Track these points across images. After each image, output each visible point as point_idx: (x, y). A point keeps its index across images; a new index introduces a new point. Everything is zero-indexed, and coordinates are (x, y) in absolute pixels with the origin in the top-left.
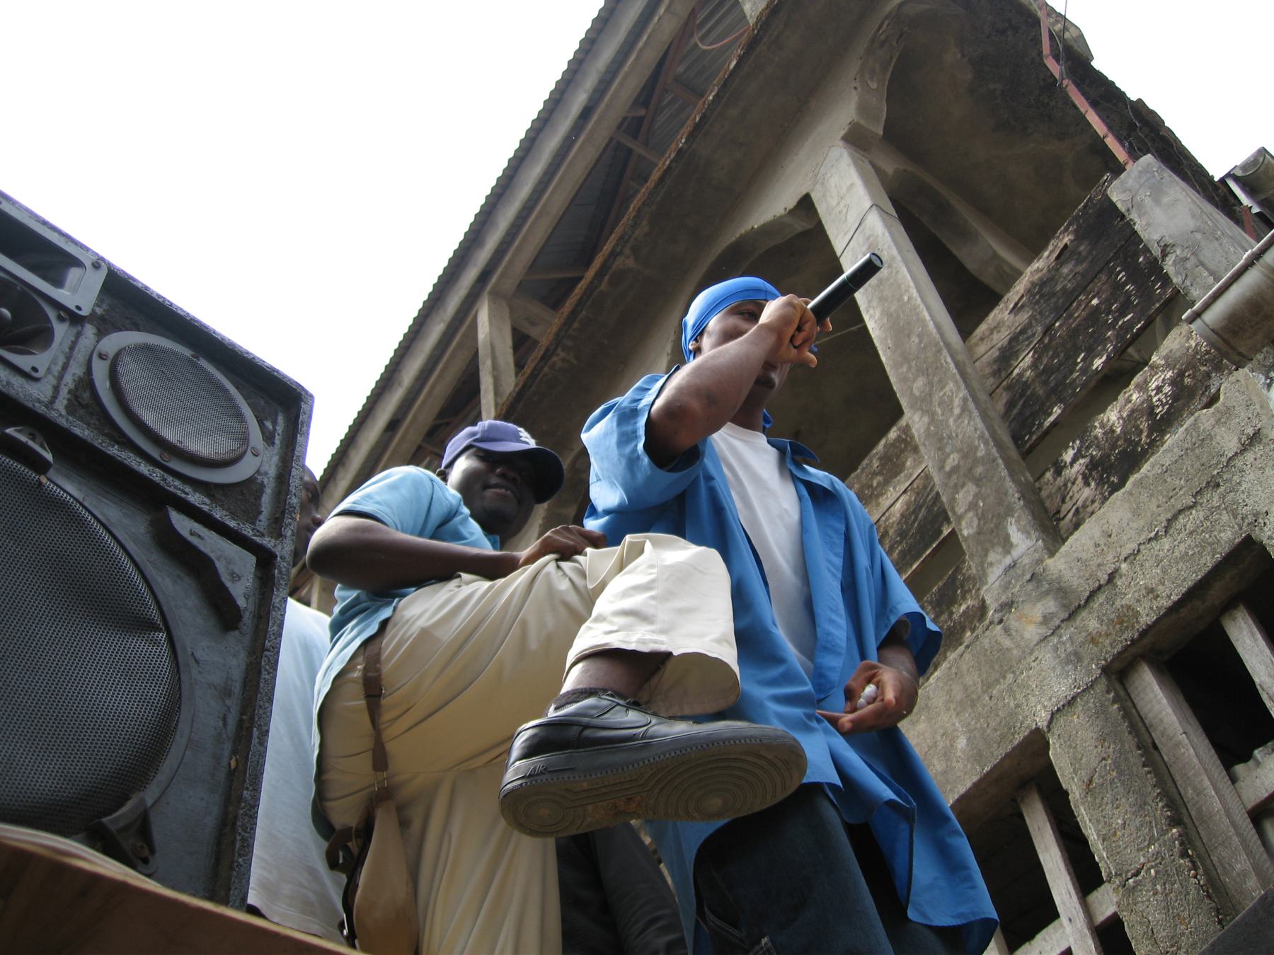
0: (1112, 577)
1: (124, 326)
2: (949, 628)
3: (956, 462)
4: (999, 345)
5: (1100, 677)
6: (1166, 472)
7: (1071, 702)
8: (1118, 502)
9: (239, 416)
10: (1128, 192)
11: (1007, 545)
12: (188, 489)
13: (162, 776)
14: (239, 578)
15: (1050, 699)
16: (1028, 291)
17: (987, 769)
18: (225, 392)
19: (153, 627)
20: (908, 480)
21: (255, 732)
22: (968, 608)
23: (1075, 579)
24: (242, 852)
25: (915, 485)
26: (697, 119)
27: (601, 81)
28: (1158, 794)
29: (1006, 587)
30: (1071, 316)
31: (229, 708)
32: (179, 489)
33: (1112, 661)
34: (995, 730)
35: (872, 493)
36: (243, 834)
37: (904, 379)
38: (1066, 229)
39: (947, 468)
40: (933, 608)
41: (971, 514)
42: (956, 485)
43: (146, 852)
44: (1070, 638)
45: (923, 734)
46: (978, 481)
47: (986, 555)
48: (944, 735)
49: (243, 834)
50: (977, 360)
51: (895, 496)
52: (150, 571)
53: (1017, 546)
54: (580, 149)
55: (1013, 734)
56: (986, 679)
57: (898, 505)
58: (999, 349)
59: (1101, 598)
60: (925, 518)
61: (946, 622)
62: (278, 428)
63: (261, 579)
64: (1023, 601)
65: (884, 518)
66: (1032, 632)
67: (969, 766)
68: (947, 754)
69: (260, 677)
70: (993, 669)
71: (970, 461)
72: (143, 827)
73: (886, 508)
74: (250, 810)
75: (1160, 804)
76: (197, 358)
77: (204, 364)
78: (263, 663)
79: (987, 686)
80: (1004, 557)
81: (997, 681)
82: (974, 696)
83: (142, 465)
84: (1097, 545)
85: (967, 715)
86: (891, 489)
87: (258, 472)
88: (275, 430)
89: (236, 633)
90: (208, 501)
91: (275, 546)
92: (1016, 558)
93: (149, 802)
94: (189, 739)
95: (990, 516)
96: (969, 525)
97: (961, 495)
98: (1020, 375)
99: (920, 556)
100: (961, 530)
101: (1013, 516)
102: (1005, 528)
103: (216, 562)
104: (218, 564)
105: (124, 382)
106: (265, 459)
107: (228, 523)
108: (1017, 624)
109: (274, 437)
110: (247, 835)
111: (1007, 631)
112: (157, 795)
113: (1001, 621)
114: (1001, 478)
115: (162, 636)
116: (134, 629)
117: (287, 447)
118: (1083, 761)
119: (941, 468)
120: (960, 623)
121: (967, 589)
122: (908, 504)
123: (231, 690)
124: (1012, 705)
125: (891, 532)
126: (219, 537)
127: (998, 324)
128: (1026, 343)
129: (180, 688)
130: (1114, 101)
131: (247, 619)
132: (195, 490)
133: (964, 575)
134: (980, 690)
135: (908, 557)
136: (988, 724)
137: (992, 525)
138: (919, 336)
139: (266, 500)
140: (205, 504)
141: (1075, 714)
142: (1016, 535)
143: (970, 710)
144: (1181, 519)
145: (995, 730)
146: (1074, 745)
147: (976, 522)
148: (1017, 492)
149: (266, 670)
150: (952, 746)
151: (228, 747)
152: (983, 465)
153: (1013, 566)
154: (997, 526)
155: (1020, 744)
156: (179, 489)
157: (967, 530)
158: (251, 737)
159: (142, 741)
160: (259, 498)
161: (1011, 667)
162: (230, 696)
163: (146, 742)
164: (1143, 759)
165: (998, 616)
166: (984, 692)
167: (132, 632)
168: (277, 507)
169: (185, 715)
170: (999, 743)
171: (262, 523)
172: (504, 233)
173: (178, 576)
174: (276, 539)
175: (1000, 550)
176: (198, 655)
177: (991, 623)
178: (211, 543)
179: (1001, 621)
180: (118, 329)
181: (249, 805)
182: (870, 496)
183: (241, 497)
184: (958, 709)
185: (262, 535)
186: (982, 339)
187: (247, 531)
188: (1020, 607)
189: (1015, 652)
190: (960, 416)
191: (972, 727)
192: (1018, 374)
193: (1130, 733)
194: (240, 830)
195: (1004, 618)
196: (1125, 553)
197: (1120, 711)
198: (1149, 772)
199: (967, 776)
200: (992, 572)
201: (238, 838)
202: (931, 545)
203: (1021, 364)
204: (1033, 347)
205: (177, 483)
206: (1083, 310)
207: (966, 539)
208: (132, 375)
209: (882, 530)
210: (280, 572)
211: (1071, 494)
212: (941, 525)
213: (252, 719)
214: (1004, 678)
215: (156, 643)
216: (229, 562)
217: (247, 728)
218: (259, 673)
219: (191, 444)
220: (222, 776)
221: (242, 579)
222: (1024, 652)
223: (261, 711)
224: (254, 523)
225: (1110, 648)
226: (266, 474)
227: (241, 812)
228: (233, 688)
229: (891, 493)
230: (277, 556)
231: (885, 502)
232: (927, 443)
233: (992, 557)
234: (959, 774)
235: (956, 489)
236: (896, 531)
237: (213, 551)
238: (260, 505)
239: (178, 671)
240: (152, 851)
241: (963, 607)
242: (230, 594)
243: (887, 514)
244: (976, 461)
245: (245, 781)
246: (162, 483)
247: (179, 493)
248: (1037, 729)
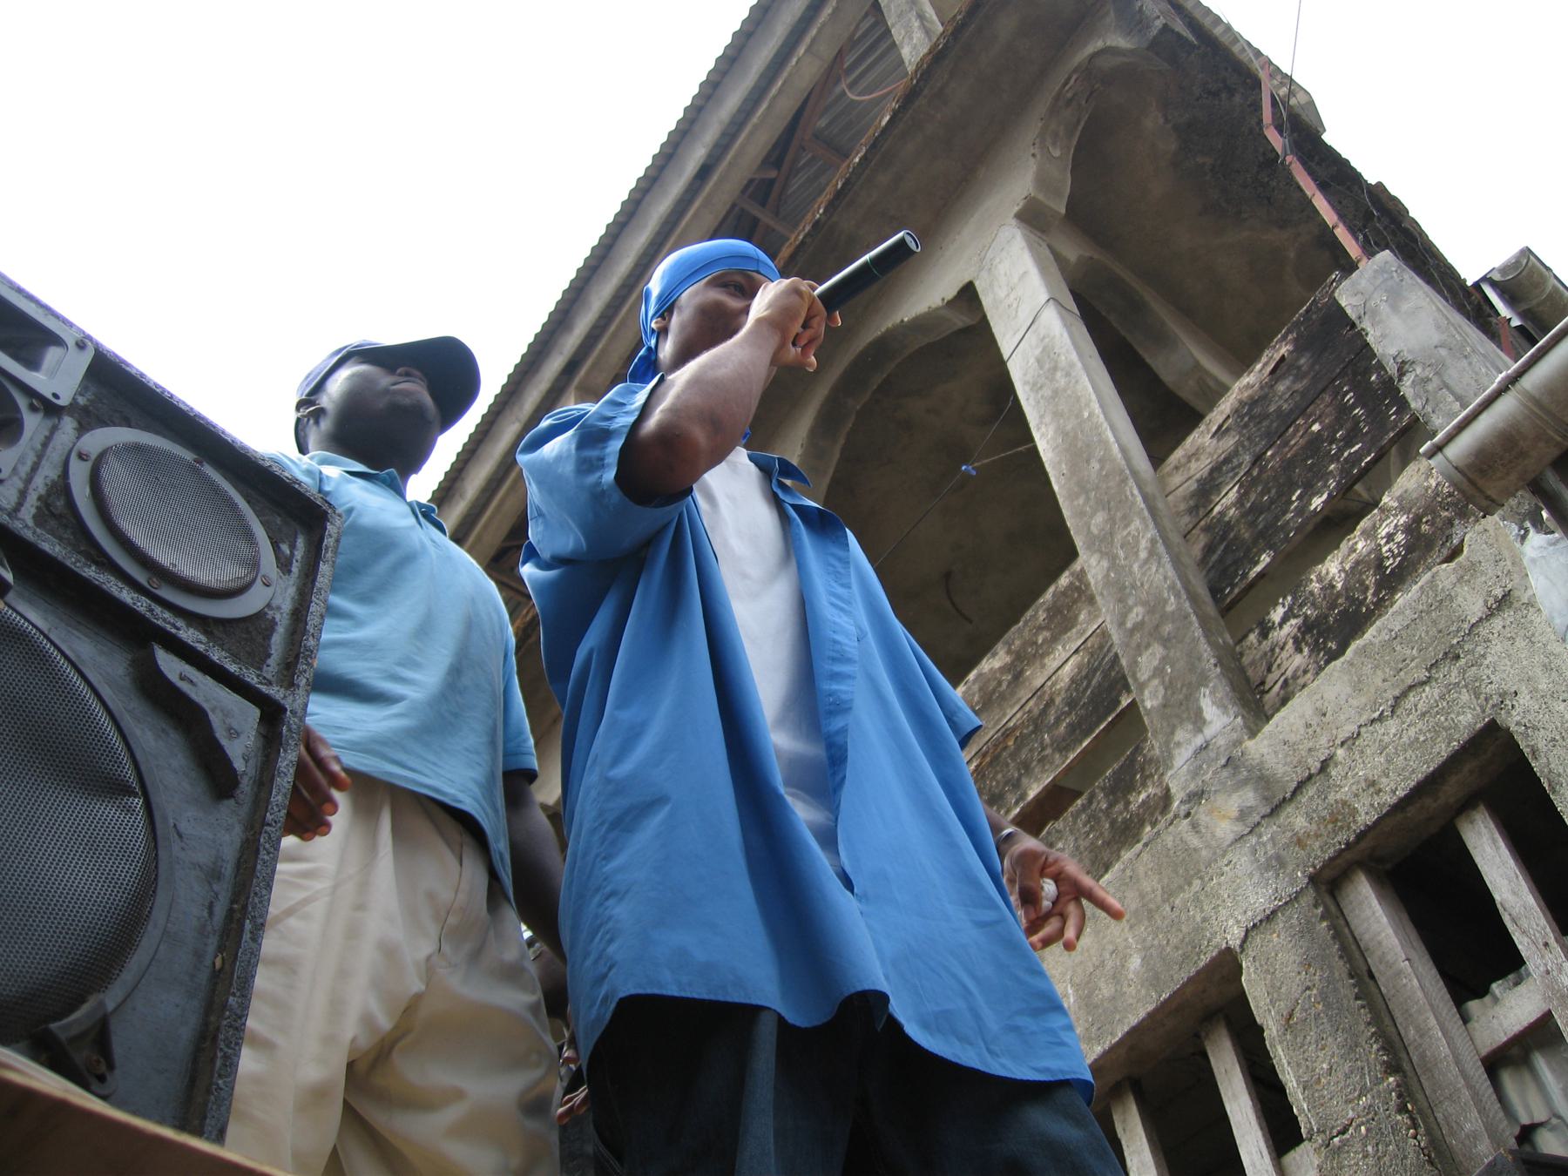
0: (1325, 765)
1: (112, 421)
2: (1125, 821)
3: (1140, 617)
4: (1198, 476)
5: (1306, 887)
6: (1395, 639)
7: (1270, 917)
8: (1336, 674)
9: (249, 536)
10: (1360, 295)
11: (1199, 722)
12: (180, 623)
13: (128, 975)
14: (238, 734)
15: (1245, 912)
16: (1236, 411)
17: (1164, 996)
18: (233, 506)
19: (127, 791)
20: (1080, 638)
21: (248, 925)
22: (1148, 797)
23: (1280, 766)
24: (222, 1072)
25: (1089, 644)
26: (839, 186)
27: (724, 134)
28: (1373, 1034)
29: (1196, 773)
30: (1286, 444)
31: (217, 894)
32: (169, 623)
33: (1322, 868)
34: (1177, 948)
35: (1037, 651)
36: (226, 1050)
37: (1080, 514)
38: (1284, 338)
39: (1129, 625)
40: (1106, 796)
41: (1156, 682)
42: (1139, 646)
43: (103, 1068)
44: (1272, 839)
45: (1088, 951)
46: (1166, 642)
47: (1173, 733)
48: (1114, 951)
49: (226, 1050)
50: (1170, 493)
51: (1064, 656)
52: (127, 721)
53: (1210, 723)
54: (695, 215)
55: (1198, 954)
56: (1168, 885)
57: (1068, 667)
58: (1198, 481)
59: (1311, 791)
60: (1100, 684)
61: (1121, 813)
62: (296, 553)
63: (265, 737)
64: (1215, 791)
65: (1049, 683)
66: (1225, 829)
67: (1143, 992)
68: (1116, 977)
69: (257, 858)
70: (1177, 873)
71: (1157, 616)
72: (100, 1036)
73: (1052, 671)
74: (235, 1021)
75: (1375, 1046)
76: (200, 463)
77: (209, 470)
78: (262, 840)
79: (1168, 894)
80: (1195, 736)
81: (1181, 888)
82: (1152, 906)
83: (125, 591)
84: (1308, 726)
85: (1143, 928)
86: (1060, 647)
87: (269, 606)
88: (292, 554)
89: (232, 801)
90: (202, 638)
91: (285, 697)
92: (1208, 738)
93: (110, 1006)
94: (165, 930)
95: (1179, 686)
96: (1154, 695)
97: (1144, 657)
98: (1222, 514)
99: (1091, 731)
100: (1143, 701)
101: (1207, 686)
102: (1198, 700)
103: (210, 714)
104: (212, 717)
105: (107, 490)
106: (279, 591)
107: (227, 666)
108: (1208, 819)
109: (291, 564)
110: (230, 1051)
111: (1195, 827)
112: (119, 1000)
113: (1188, 815)
114: (1194, 638)
115: (138, 802)
116: (103, 792)
117: (307, 576)
118: (1283, 990)
119: (1121, 624)
120: (1138, 815)
121: (1148, 773)
122: (1080, 667)
123: (220, 872)
124: (1198, 919)
125: (1058, 700)
126: (216, 683)
127: (1198, 449)
128: (1231, 474)
129: (156, 867)
130: (1349, 183)
131: (246, 786)
132: (189, 625)
133: (1145, 756)
134: (1159, 898)
135: (1078, 732)
136: (1168, 940)
137: (1181, 697)
138: (1101, 461)
139: (277, 641)
140: (201, 642)
141: (1274, 932)
142: (1209, 710)
143: (1146, 923)
144: (1412, 698)
145: (1177, 948)
146: (1272, 970)
147: (1161, 691)
148: (1214, 656)
149: (265, 849)
150: (1123, 966)
151: (213, 942)
152: (1173, 622)
153: (1204, 748)
154: (1187, 698)
155: (1207, 966)
156: (169, 623)
157: (1150, 701)
158: (242, 931)
159: (105, 931)
160: (268, 637)
161: (1199, 871)
162: (219, 878)
163: (110, 932)
164: (1356, 990)
165: (1184, 808)
166: (1164, 901)
167: (100, 796)
168: (291, 650)
169: (161, 899)
170: (1183, 962)
171: (270, 669)
172: (597, 316)
173: (163, 730)
174: (287, 689)
175: (1190, 727)
176: (183, 826)
177: (1176, 816)
178: (205, 691)
179: (1188, 815)
180: (103, 422)
181: (236, 1015)
182: (1034, 656)
183: (244, 636)
184: (1132, 921)
185: (270, 683)
186: (1177, 468)
187: (251, 677)
188: (1212, 798)
189: (1204, 853)
190: (1146, 561)
191: (1148, 944)
192: (1219, 513)
193: (1341, 957)
194: (222, 1045)
195: (1192, 812)
196: (1342, 736)
197: (1329, 930)
198: (1363, 1007)
199: (1140, 1005)
200: (1179, 754)
201: (219, 1054)
202: (1105, 719)
203: (1224, 500)
204: (1239, 481)
205: (167, 615)
206: (1301, 437)
207: (1148, 712)
208: (117, 479)
209: (1047, 697)
210: (290, 730)
211: (1279, 661)
212: (1119, 694)
213: (245, 907)
214: (1190, 884)
215: (129, 810)
216: (227, 714)
217: (238, 920)
218: (257, 852)
219: (187, 568)
220: (203, 977)
221: (242, 736)
222: (1215, 853)
223: (256, 900)
224: (260, 669)
225: (1320, 852)
226: (279, 608)
227: (225, 1023)
228: (223, 870)
229: (1060, 653)
230: (286, 710)
231: (1052, 663)
232: (1105, 593)
233: (1180, 735)
234: (1131, 1001)
235: (1140, 649)
236: (1063, 699)
237: (207, 701)
238: (269, 646)
239: (156, 847)
240: (111, 1066)
241: (1143, 796)
242: (227, 755)
243: (1054, 678)
244: (1164, 617)
245: (231, 984)
246: (148, 615)
247: (168, 627)
248: (1228, 949)
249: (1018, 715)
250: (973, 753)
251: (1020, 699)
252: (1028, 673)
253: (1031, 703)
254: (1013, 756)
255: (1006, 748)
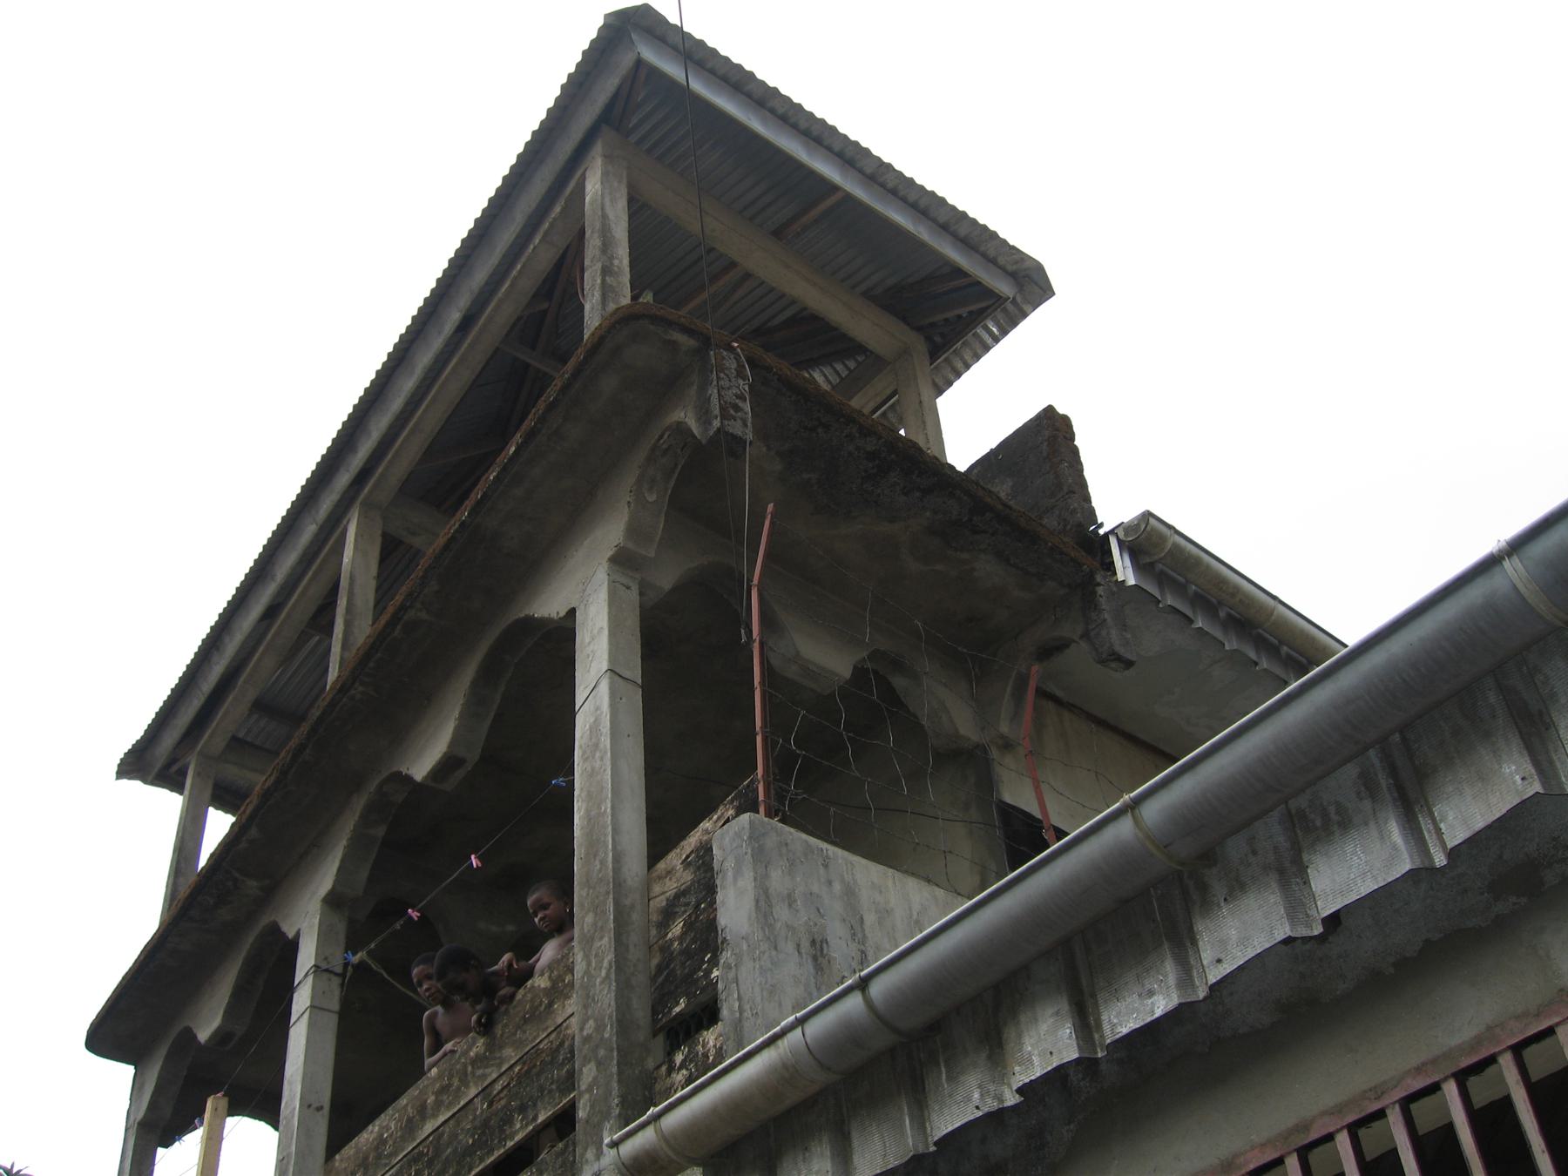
4: (668, 894)
26: (479, 497)
27: (407, 404)
38: (732, 801)
39: (585, 1033)
54: (454, 369)
73: (568, 1015)
127: (672, 869)
130: (950, 489)
172: (375, 444)
186: (660, 878)
243: (568, 1022)
249: (546, 1041)
250: (518, 1057)
251: (547, 1028)
252: (556, 1006)
253: (553, 1036)
254: (538, 1075)
255: (535, 1066)
